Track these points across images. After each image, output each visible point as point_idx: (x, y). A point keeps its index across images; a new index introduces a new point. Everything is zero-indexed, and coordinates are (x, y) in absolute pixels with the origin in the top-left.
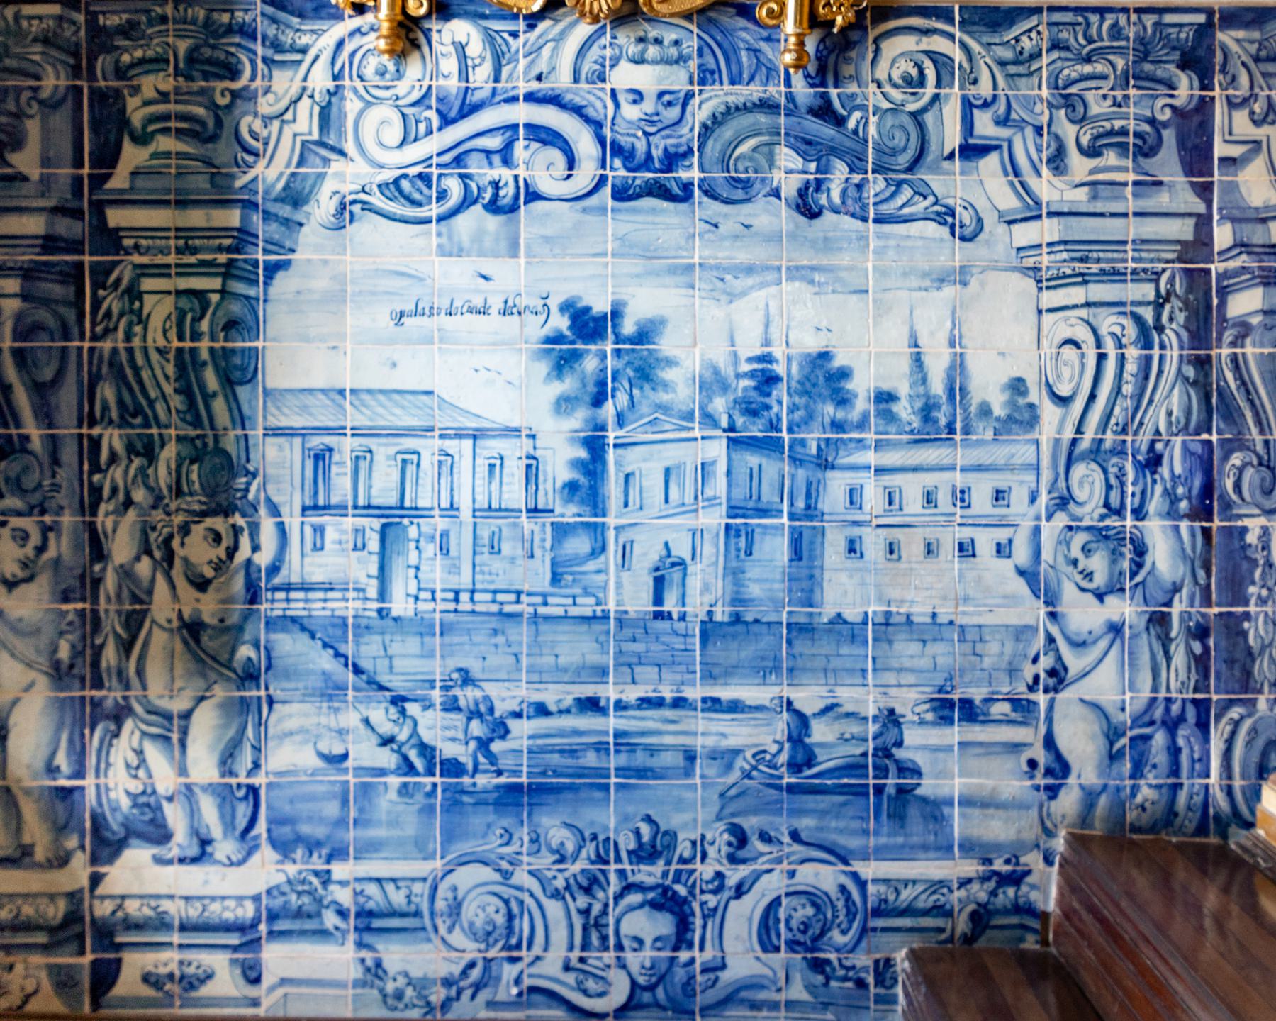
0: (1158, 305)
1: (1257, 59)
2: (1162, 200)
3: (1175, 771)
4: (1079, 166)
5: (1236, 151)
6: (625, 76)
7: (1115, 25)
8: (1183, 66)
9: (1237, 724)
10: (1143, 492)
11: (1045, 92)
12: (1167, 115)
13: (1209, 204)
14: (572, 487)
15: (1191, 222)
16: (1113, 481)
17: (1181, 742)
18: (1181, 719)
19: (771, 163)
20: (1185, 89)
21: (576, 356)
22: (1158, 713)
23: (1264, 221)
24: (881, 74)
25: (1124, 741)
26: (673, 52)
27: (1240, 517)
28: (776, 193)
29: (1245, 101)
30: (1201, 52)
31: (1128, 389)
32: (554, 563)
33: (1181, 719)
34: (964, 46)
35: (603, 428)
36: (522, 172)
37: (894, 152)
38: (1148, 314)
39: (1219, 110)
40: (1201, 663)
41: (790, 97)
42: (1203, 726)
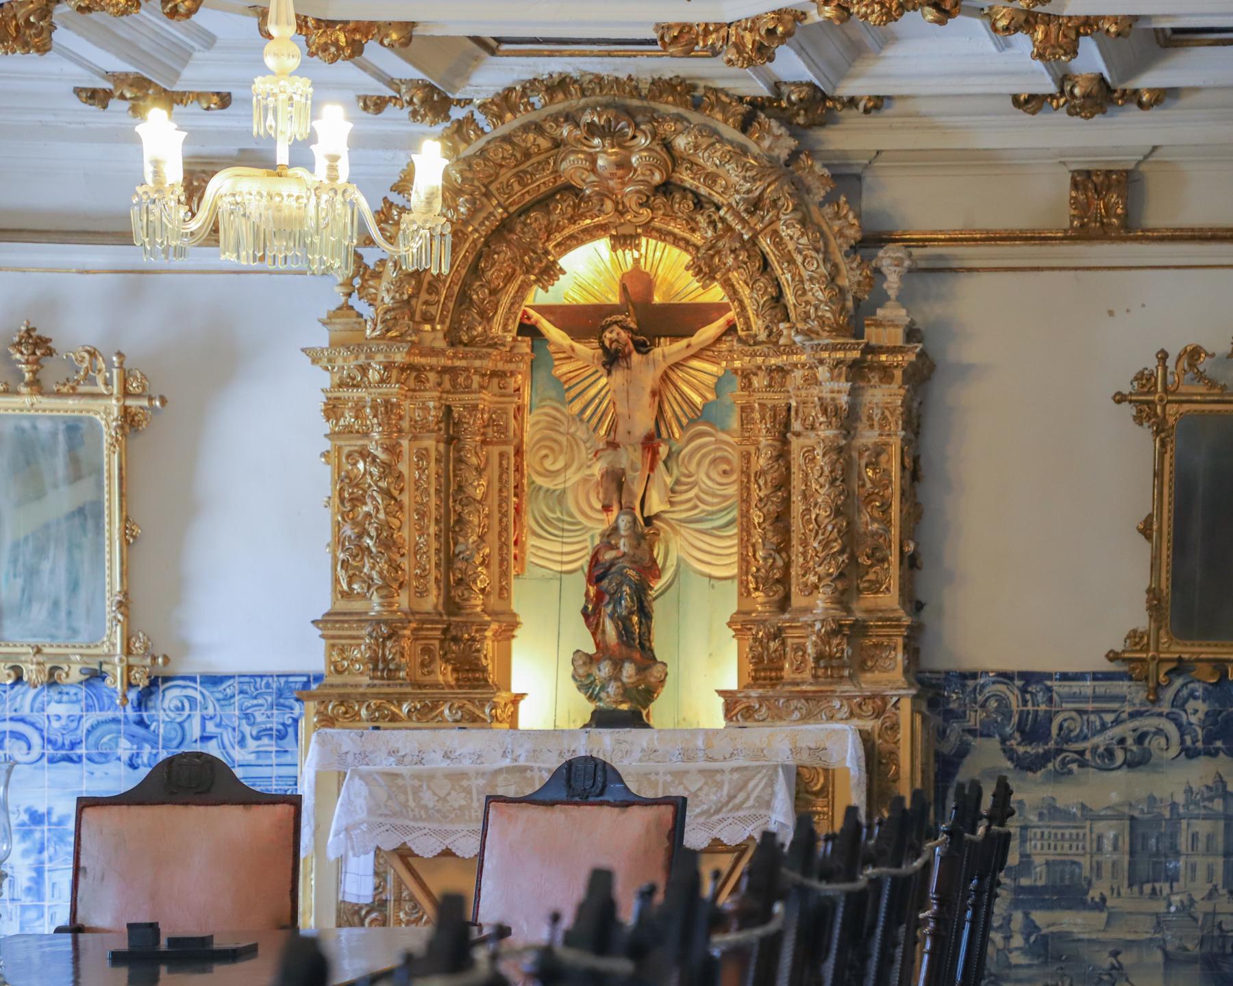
4: (252, 744)
6: (53, 709)
11: (237, 712)
14: (29, 889)
19: (117, 745)
21: (30, 832)
24: (165, 705)
26: (74, 698)
28: (119, 759)
32: (21, 923)
34: (202, 693)
35: (43, 863)
36: (8, 752)
37: (171, 740)
41: (126, 717)
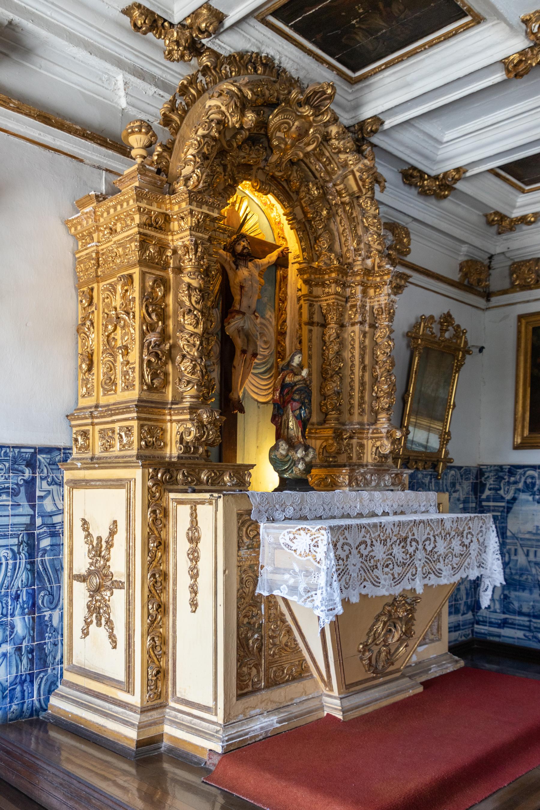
0: (19, 545)
1: (49, 464)
2: (20, 510)
3: (23, 698)
5: (43, 494)
7: (5, 452)
8: (27, 466)
9: (42, 678)
10: (14, 608)
12: (22, 482)
13: (35, 511)
15: (29, 517)
16: (4, 605)
17: (25, 688)
18: (25, 680)
20: (28, 473)
22: (18, 680)
23: (51, 516)
25: (7, 691)
27: (43, 612)
29: (46, 477)
30: (33, 462)
31: (9, 574)
33: (25, 680)
38: (15, 548)
39: (38, 480)
40: (31, 661)
42: (32, 682)
